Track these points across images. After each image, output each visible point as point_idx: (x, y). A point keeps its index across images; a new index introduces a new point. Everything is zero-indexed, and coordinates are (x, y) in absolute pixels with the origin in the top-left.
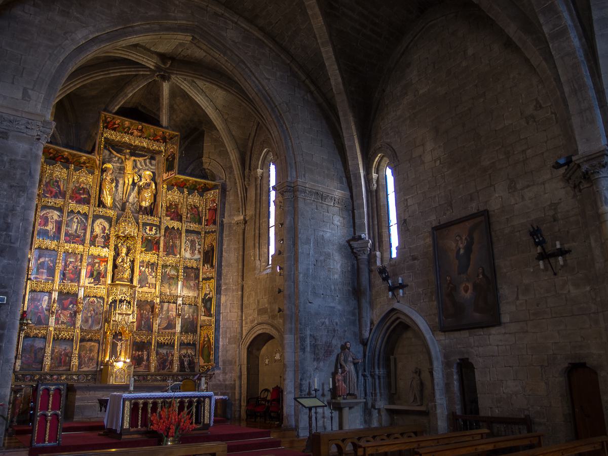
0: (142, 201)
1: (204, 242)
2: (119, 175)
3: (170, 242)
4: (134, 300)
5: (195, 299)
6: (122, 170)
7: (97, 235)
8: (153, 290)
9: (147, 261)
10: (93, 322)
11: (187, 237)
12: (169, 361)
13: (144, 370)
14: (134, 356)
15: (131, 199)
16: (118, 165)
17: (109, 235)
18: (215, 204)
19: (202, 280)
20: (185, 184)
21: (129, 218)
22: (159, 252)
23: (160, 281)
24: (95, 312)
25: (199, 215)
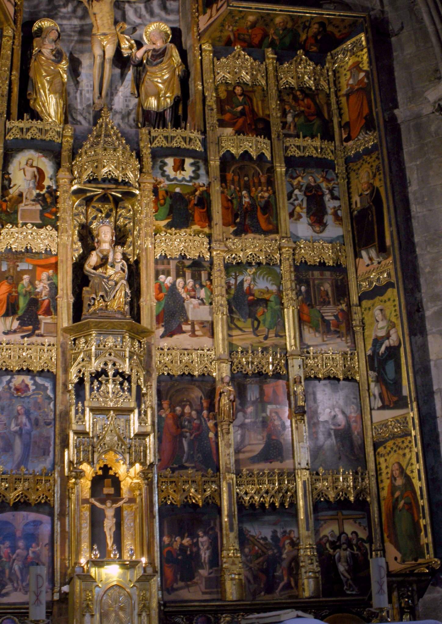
0: (147, 96)
1: (349, 188)
2: (78, 46)
3: (241, 197)
4: (148, 374)
5: (345, 359)
6: (85, 33)
7: (21, 195)
8: (206, 342)
9: (177, 254)
10: (26, 447)
11: (294, 178)
12: (285, 564)
13: (207, 597)
14: (169, 552)
15: (119, 102)
16: (76, 22)
17: (56, 191)
18: (362, 75)
19: (360, 299)
20: (266, 35)
21: (107, 136)
22: (210, 227)
23: (225, 310)
24: (32, 417)
25: (319, 114)
